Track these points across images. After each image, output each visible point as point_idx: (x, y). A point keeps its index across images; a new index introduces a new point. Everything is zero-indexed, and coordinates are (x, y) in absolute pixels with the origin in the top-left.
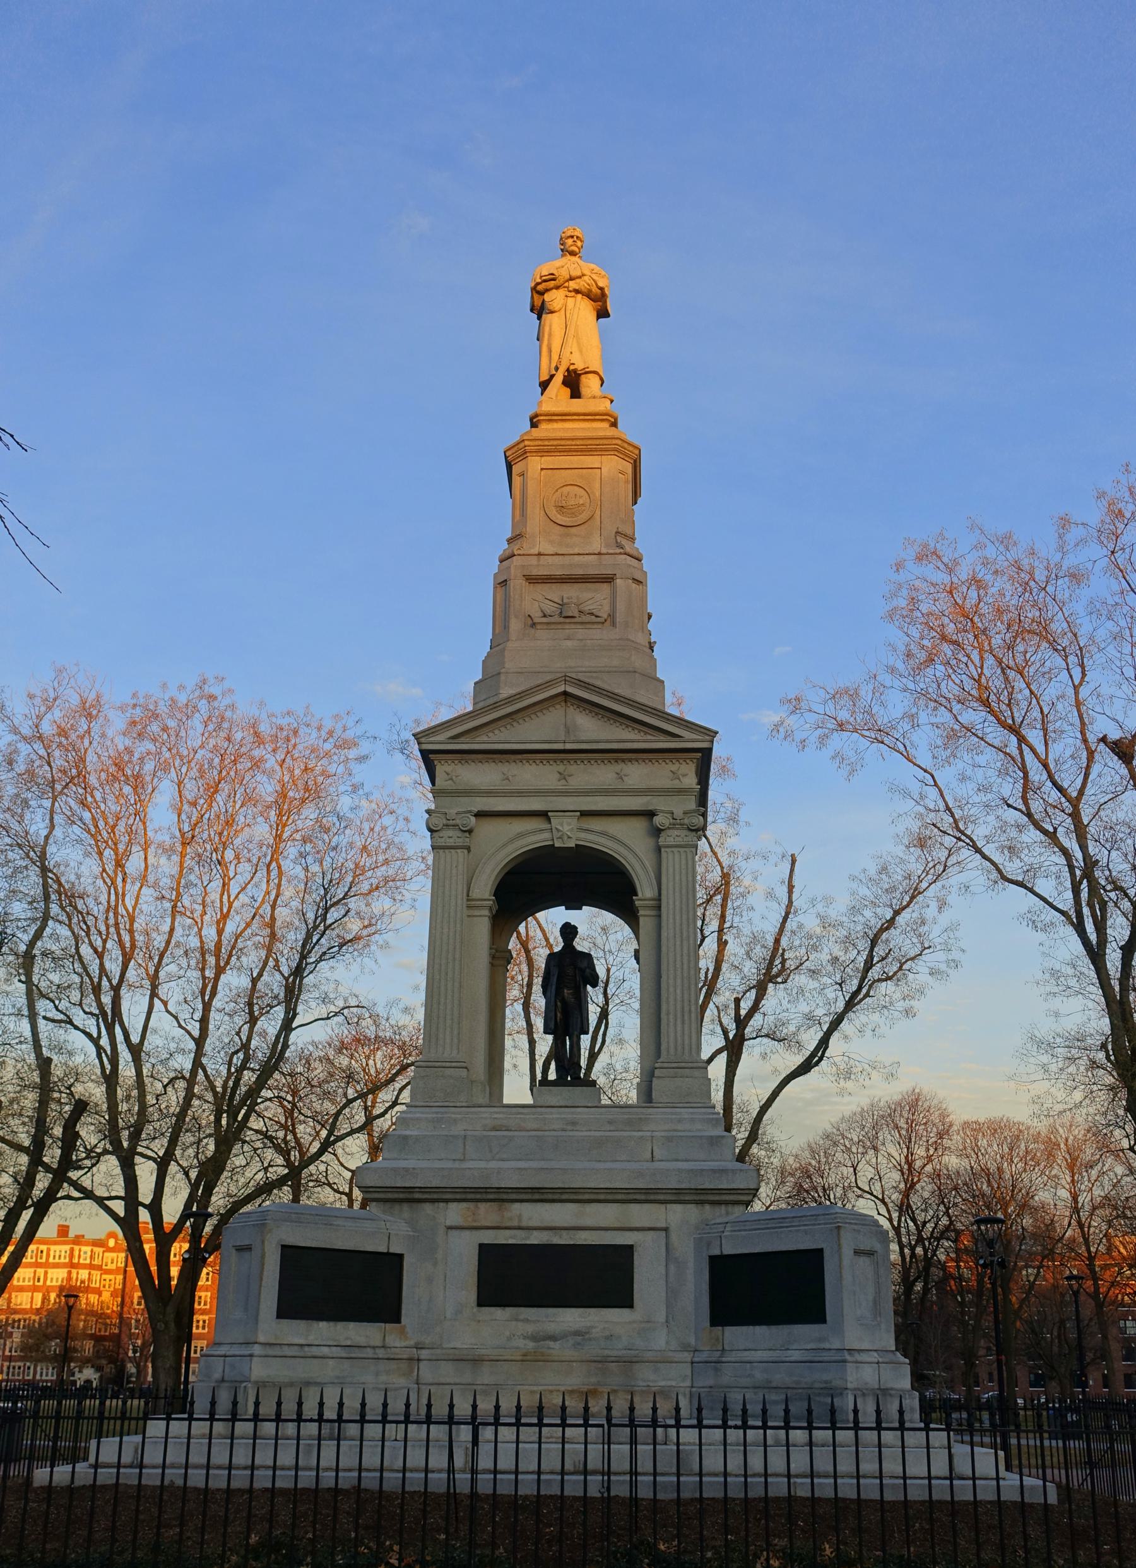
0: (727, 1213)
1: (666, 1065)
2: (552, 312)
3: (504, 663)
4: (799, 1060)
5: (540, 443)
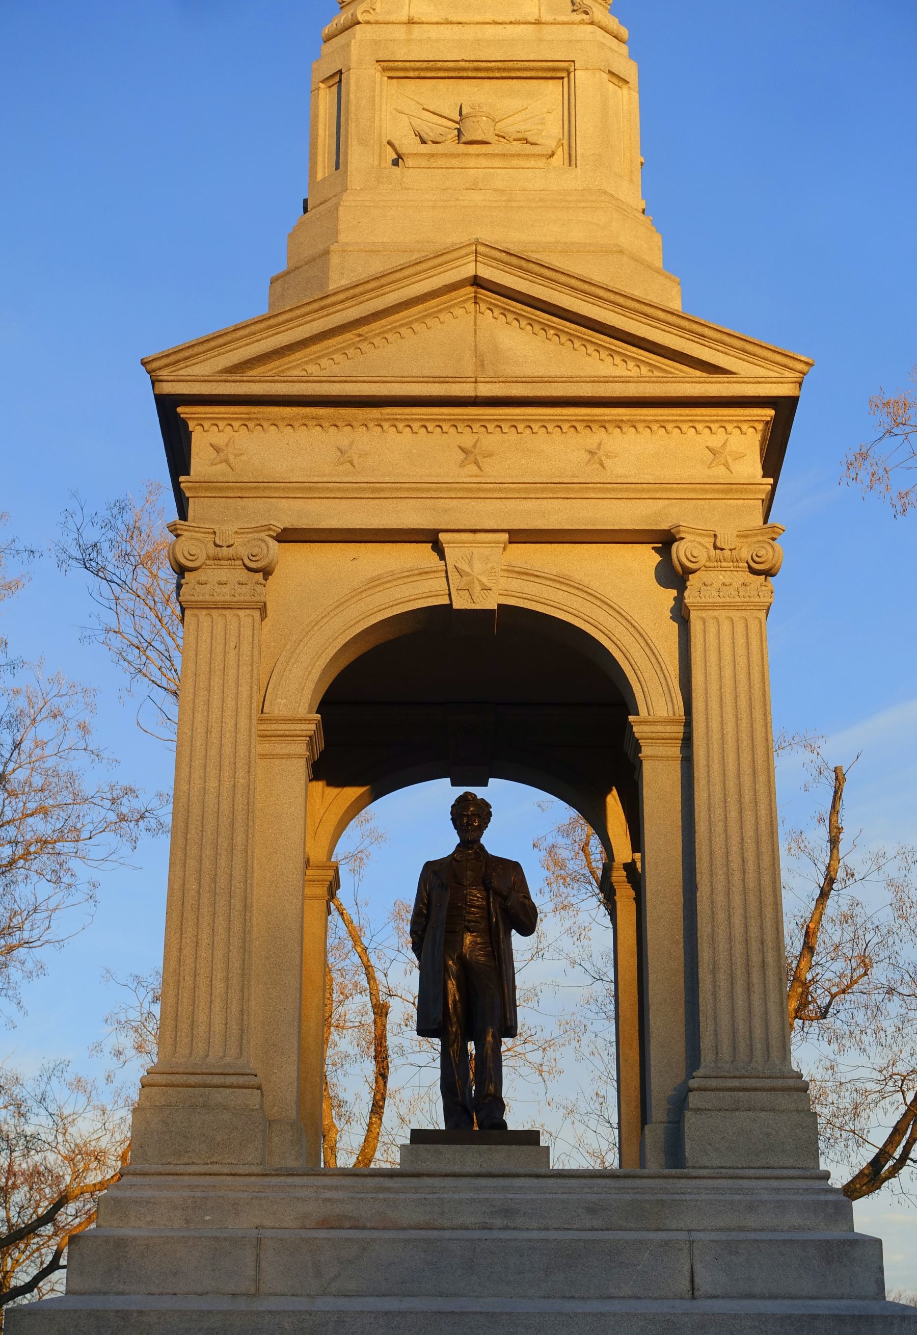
1: (713, 1083)
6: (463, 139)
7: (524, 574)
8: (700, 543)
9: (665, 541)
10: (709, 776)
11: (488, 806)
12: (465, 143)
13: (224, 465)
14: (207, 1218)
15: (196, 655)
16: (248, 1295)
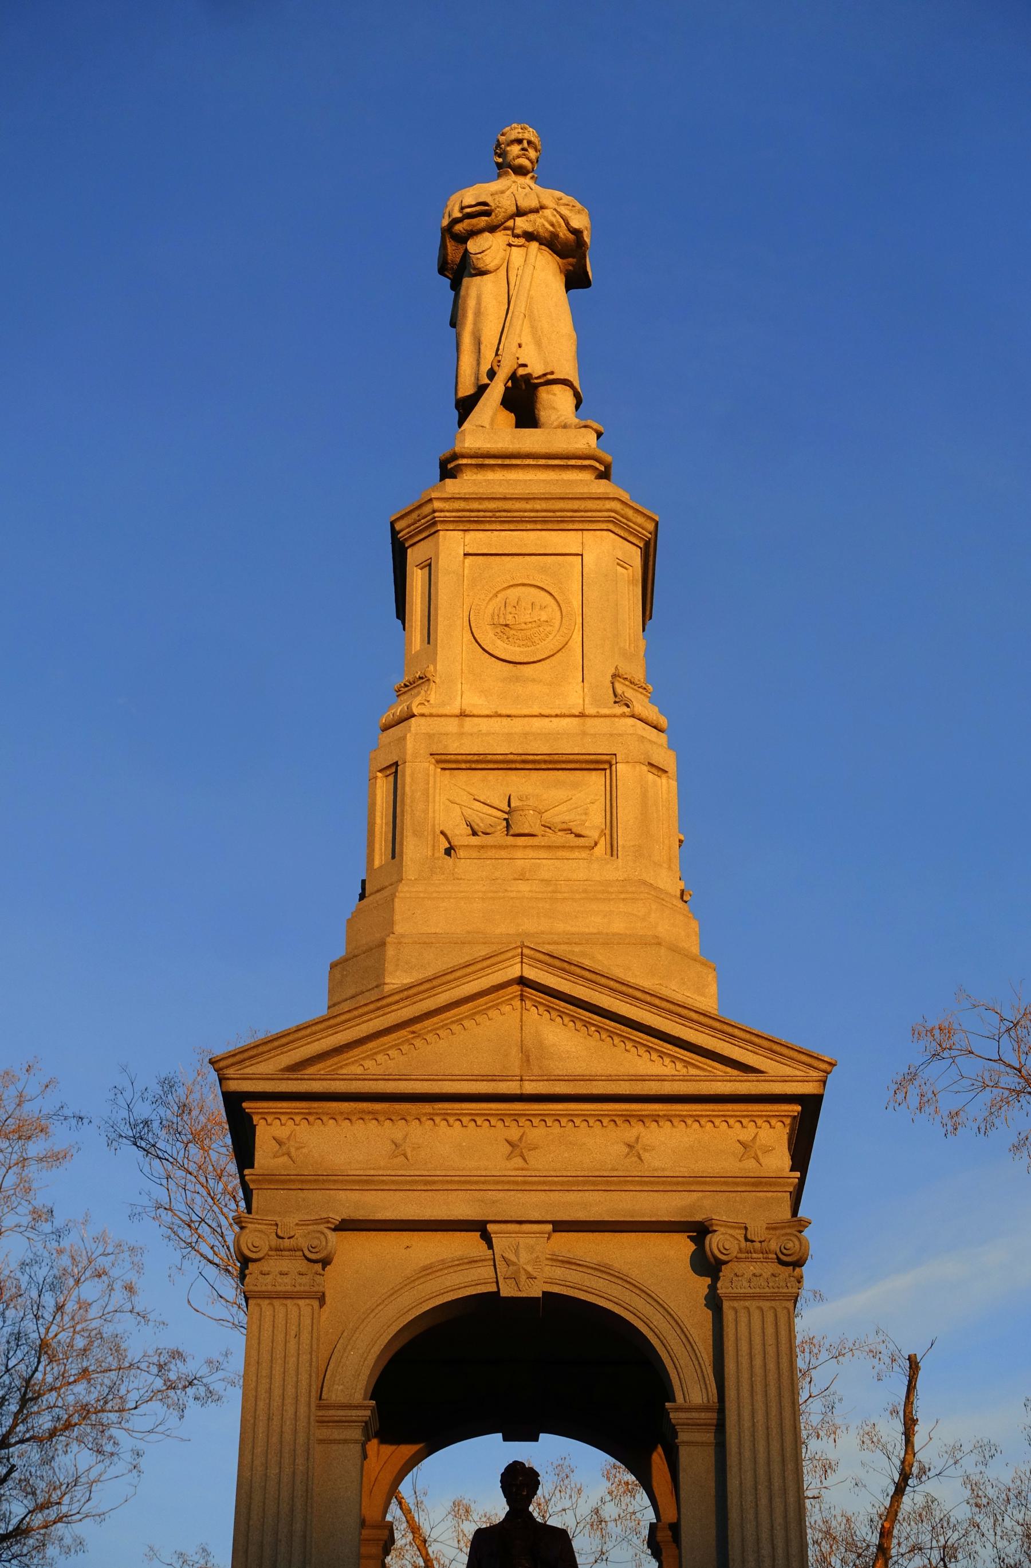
2: (483, 273)
3: (392, 923)
5: (462, 505)
6: (511, 832)
7: (568, 1262)
12: (513, 835)
13: (286, 1158)
15: (259, 1343)
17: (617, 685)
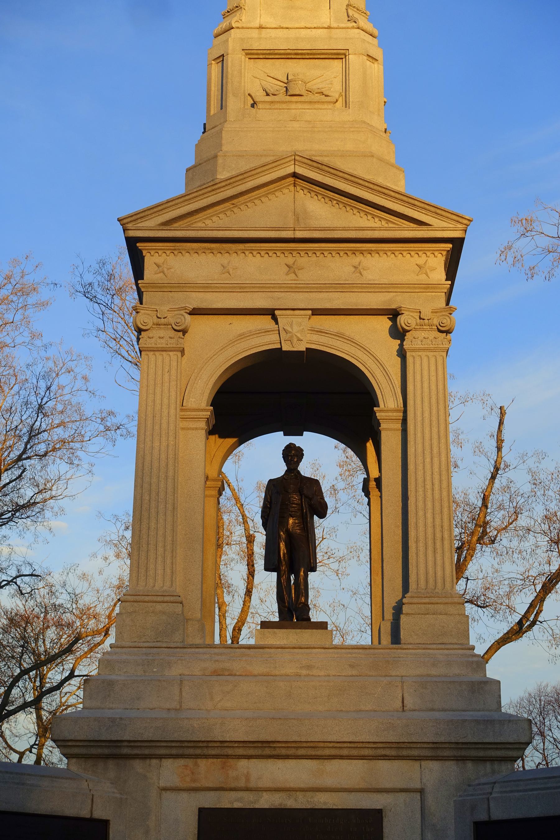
0: (493, 772)
1: (415, 600)
3: (221, 145)
4: (504, 628)
6: (289, 94)
7: (320, 332)
8: (412, 316)
9: (394, 314)
10: (415, 440)
11: (302, 450)
12: (290, 96)
13: (162, 274)
14: (155, 670)
15: (148, 376)
16: (176, 710)
17: (349, 11)
